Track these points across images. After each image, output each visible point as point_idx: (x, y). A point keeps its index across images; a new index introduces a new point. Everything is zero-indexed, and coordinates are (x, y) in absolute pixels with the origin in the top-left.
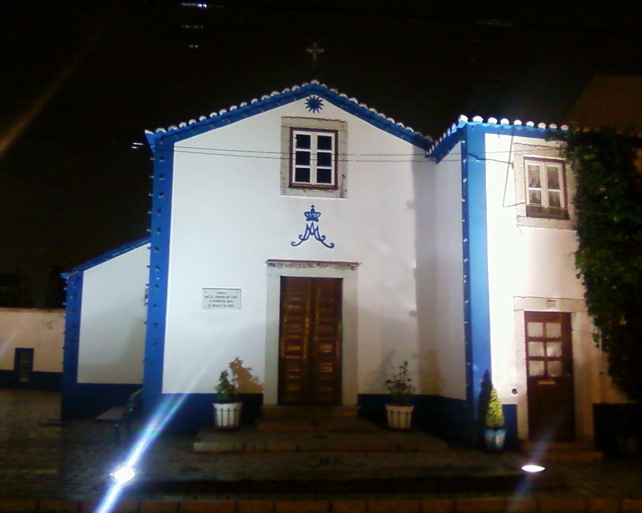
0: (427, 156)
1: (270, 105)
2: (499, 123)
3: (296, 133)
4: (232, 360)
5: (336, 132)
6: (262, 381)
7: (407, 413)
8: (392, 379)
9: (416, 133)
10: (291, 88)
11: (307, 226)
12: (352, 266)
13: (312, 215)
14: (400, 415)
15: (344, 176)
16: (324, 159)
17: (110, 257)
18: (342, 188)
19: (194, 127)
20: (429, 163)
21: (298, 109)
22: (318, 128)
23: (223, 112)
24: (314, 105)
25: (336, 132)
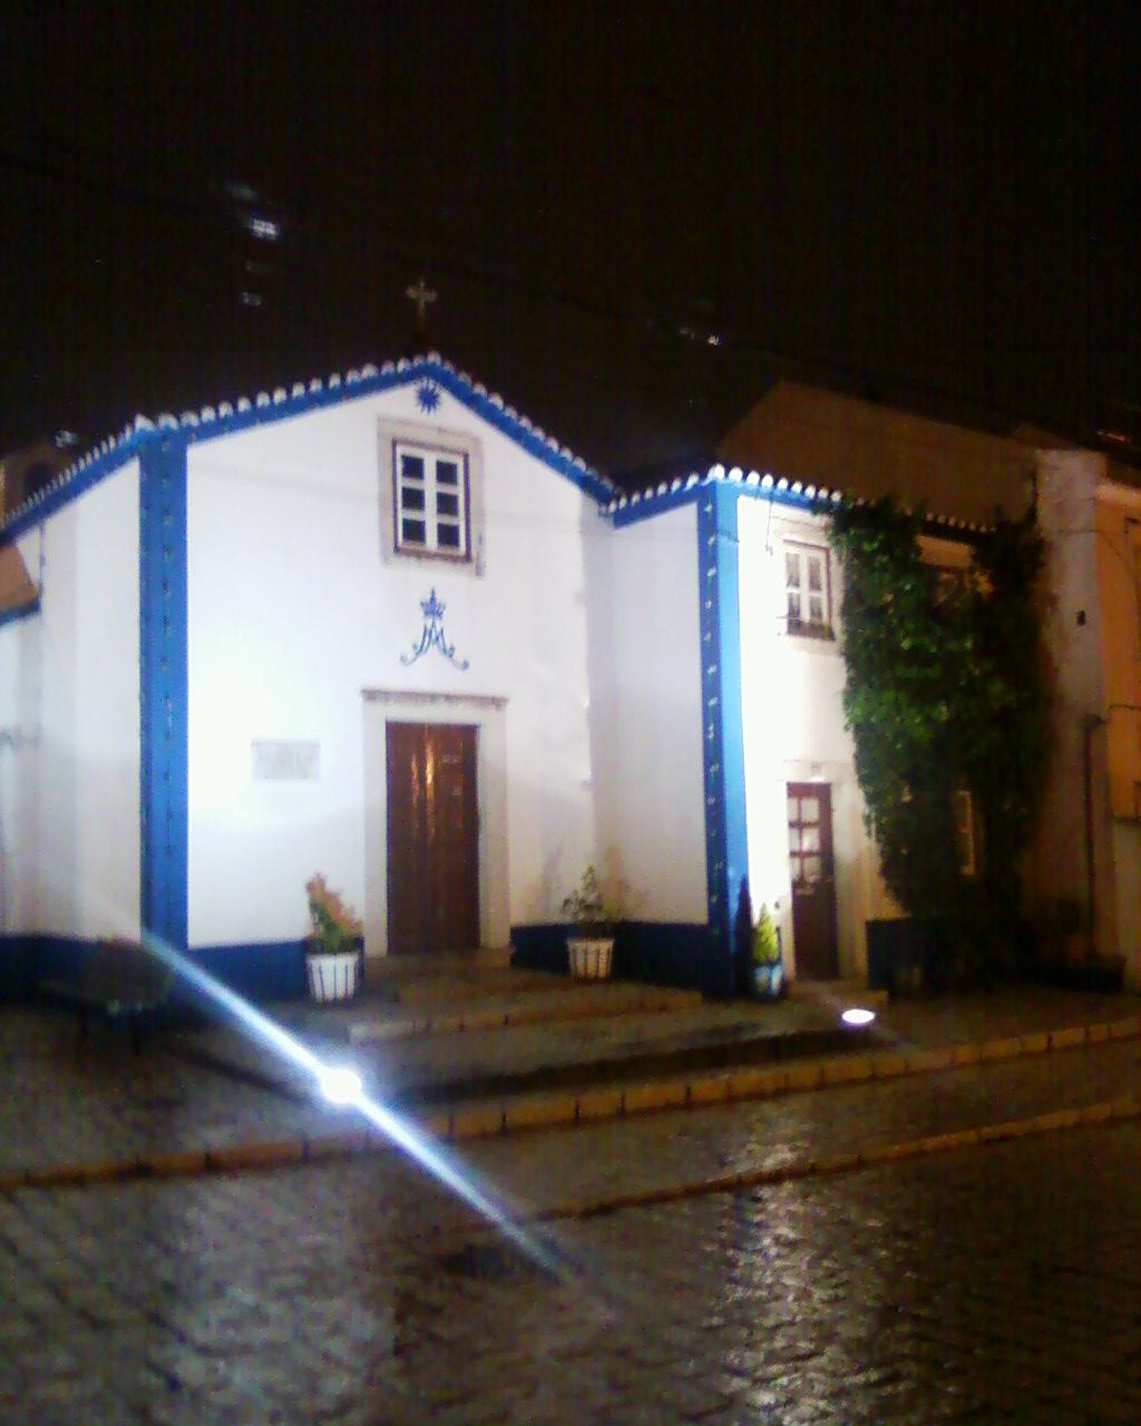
0: (606, 515)
3: (400, 451)
4: (309, 875)
9: (589, 473)
12: (497, 702)
13: (432, 608)
14: (593, 955)
15: (481, 539)
16: (446, 504)
18: (478, 559)
20: (606, 526)
21: (400, 402)
24: (428, 400)
25: (466, 457)
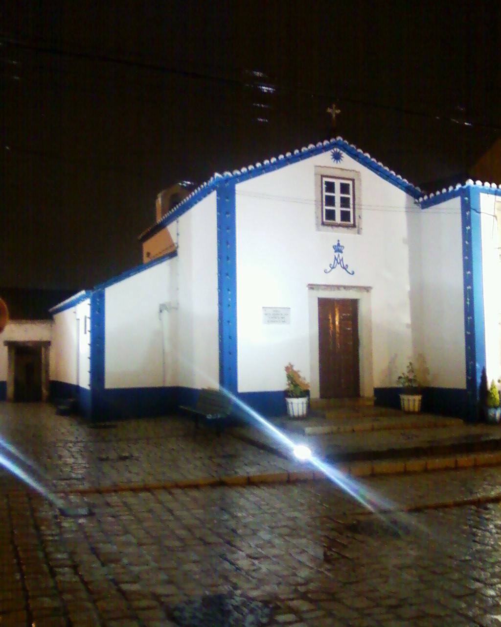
0: (415, 203)
1: (384, 176)
2: (483, 185)
3: (325, 179)
4: (287, 364)
5: (353, 180)
6: (308, 380)
7: (303, 404)
8: (402, 376)
9: (410, 184)
10: (322, 142)
11: (335, 257)
12: (367, 289)
13: (338, 249)
14: (412, 402)
15: (360, 217)
16: (345, 202)
17: (128, 276)
18: (359, 225)
19: (249, 172)
20: (418, 208)
21: (325, 159)
22: (340, 176)
23: (273, 160)
24: (337, 157)
25: (353, 180)
